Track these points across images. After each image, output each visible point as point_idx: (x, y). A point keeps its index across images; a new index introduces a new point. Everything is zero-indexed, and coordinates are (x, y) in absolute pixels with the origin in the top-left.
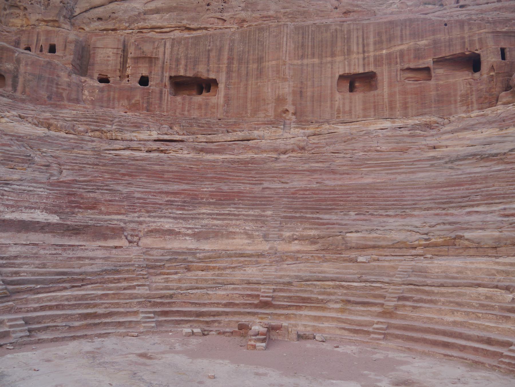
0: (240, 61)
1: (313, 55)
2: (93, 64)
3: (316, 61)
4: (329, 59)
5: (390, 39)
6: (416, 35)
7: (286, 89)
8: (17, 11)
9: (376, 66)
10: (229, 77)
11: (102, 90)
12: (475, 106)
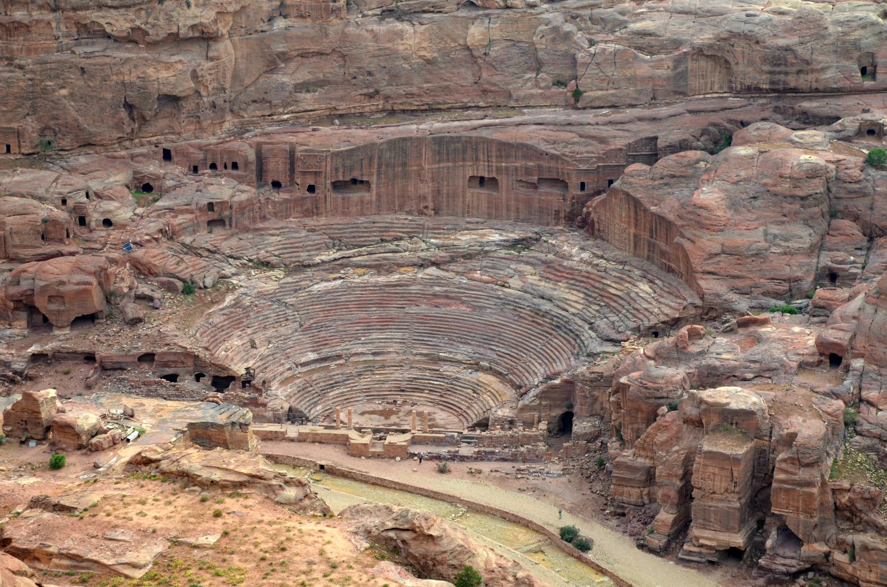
0: (387, 165)
1: (448, 160)
2: (266, 172)
3: (450, 164)
4: (461, 163)
5: (507, 157)
6: (525, 157)
7: (426, 189)
8: (191, 119)
9: (497, 173)
10: (379, 178)
11: (281, 204)
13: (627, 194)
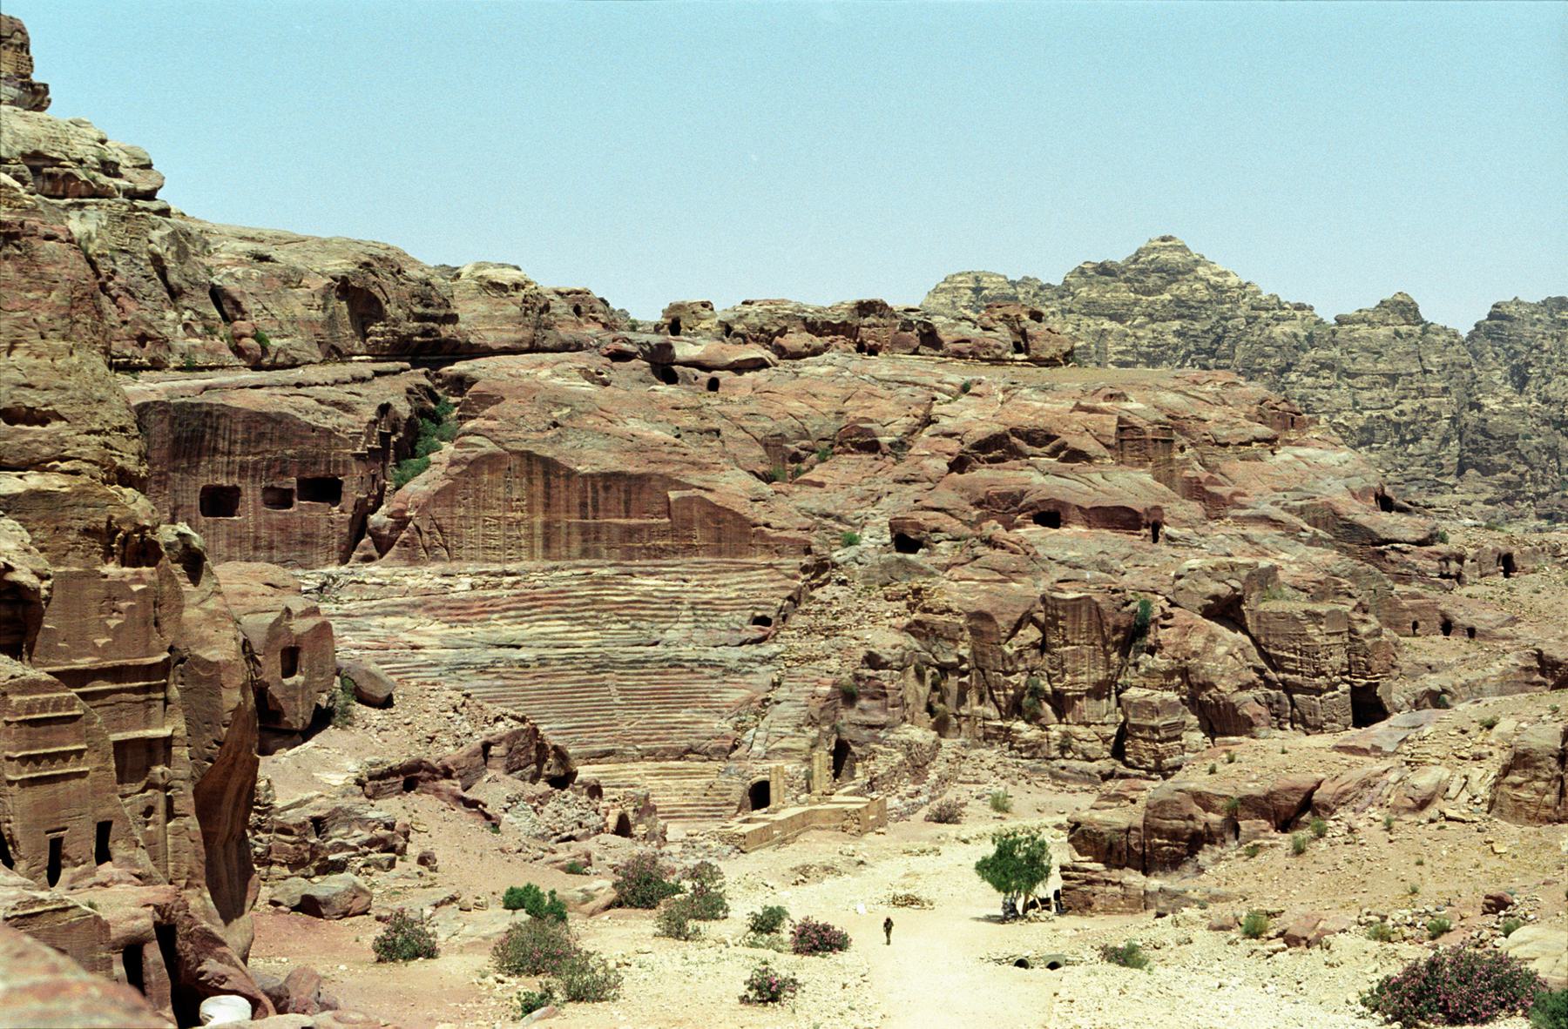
9: (240, 477)
12: (336, 554)
13: (528, 456)
